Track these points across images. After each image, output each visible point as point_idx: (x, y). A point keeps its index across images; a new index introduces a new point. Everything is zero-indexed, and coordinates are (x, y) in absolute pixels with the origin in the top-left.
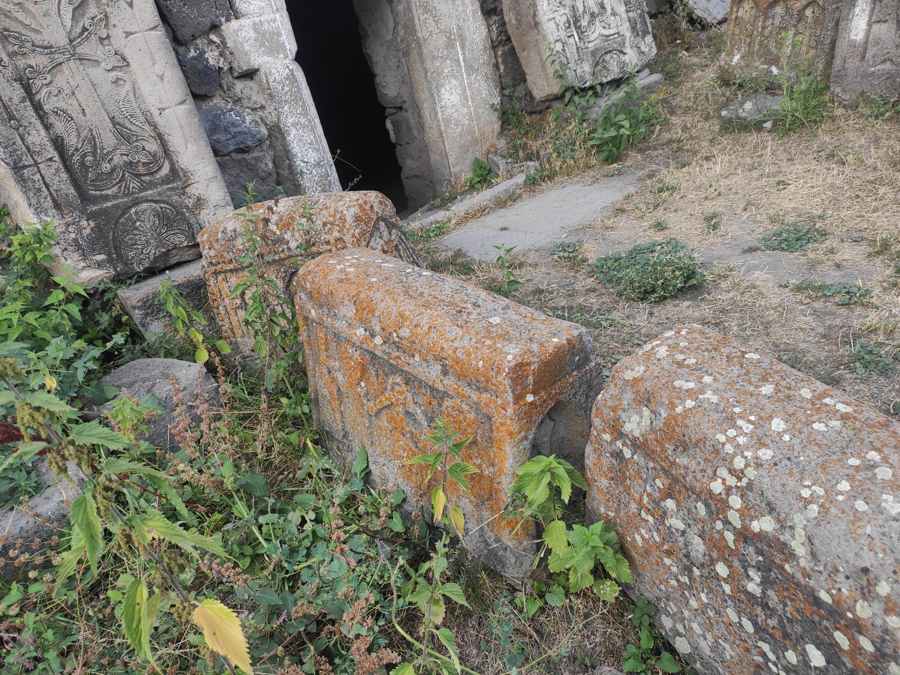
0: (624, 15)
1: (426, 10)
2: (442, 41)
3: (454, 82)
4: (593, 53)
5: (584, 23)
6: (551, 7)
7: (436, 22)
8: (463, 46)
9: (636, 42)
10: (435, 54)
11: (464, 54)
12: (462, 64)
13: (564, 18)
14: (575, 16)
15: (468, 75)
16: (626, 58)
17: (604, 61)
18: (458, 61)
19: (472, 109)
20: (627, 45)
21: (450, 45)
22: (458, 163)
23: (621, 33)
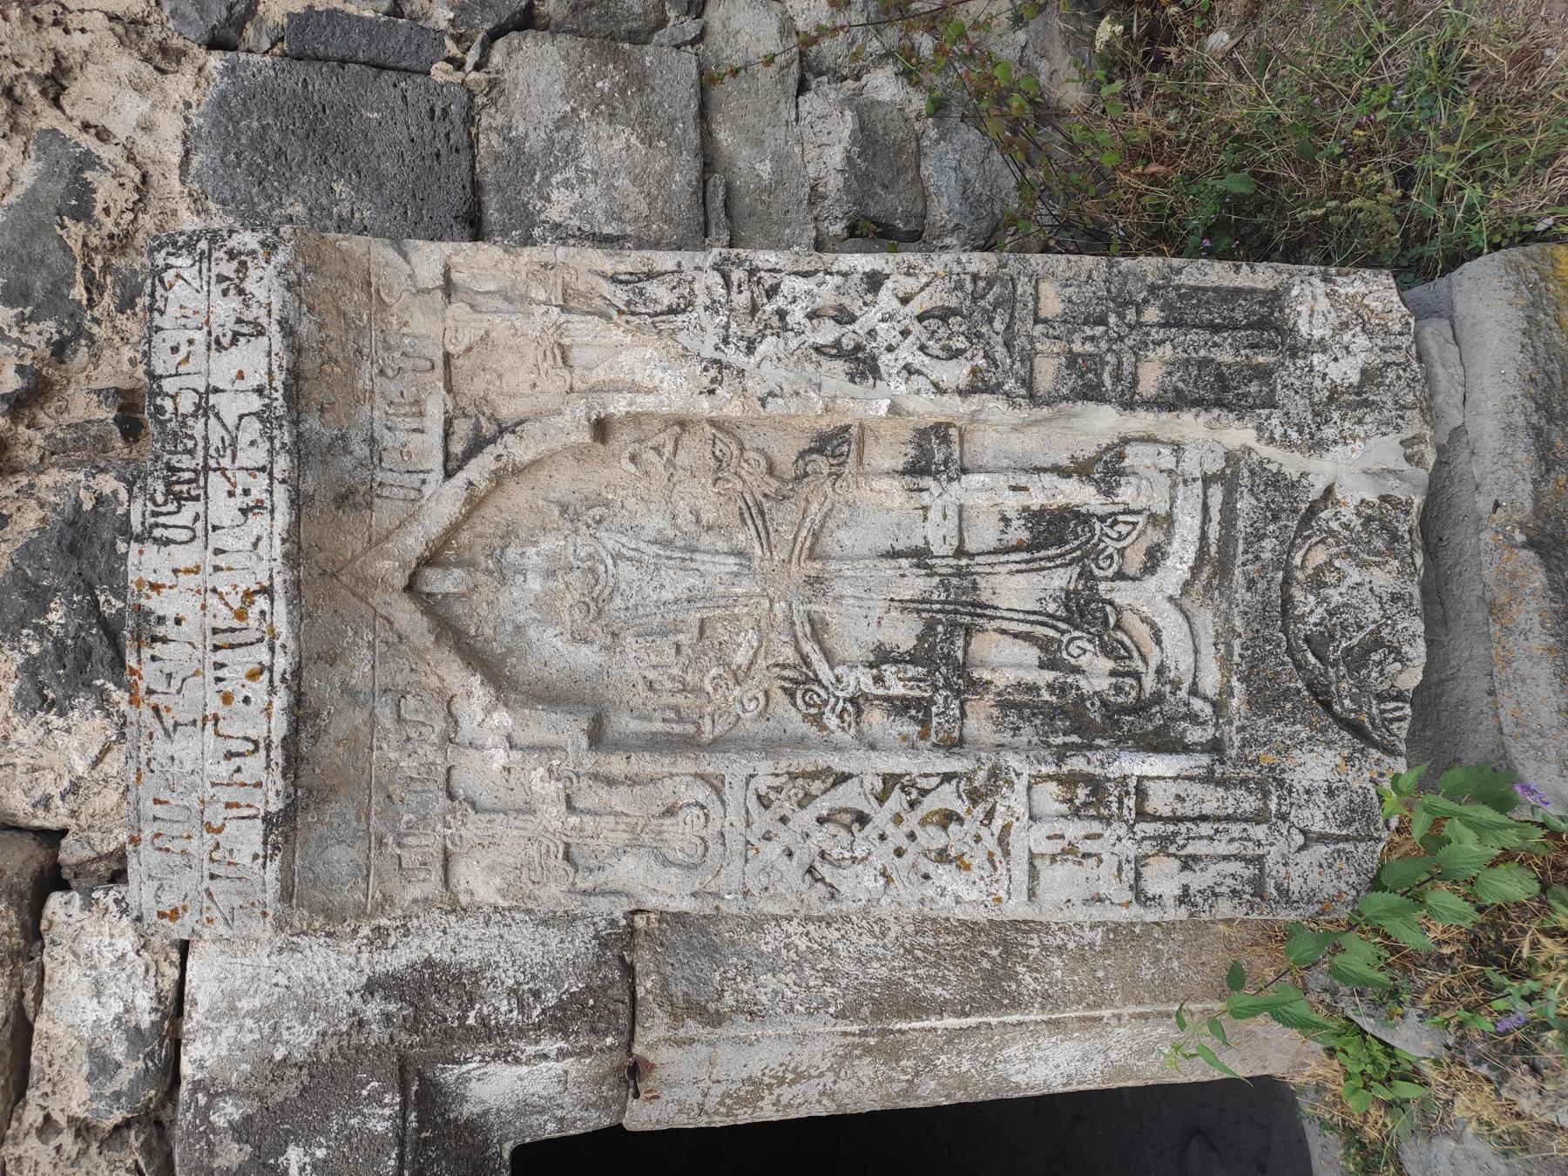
0: (1142, 421)
1: (753, 1100)
2: (866, 1068)
3: (1015, 1050)
4: (1265, 699)
5: (1096, 674)
6: (978, 860)
7: (799, 1077)
8: (917, 1006)
9: (1299, 406)
10: (896, 1087)
11: (941, 1009)
12: (972, 1021)
13: (1049, 797)
14: (1050, 714)
15: (1016, 1004)
16: (1356, 492)
17: (1317, 643)
18: (952, 1036)
19: (1132, 1009)
20: (1291, 463)
21: (891, 1051)
22: (1263, 1058)
23: (1215, 465)
